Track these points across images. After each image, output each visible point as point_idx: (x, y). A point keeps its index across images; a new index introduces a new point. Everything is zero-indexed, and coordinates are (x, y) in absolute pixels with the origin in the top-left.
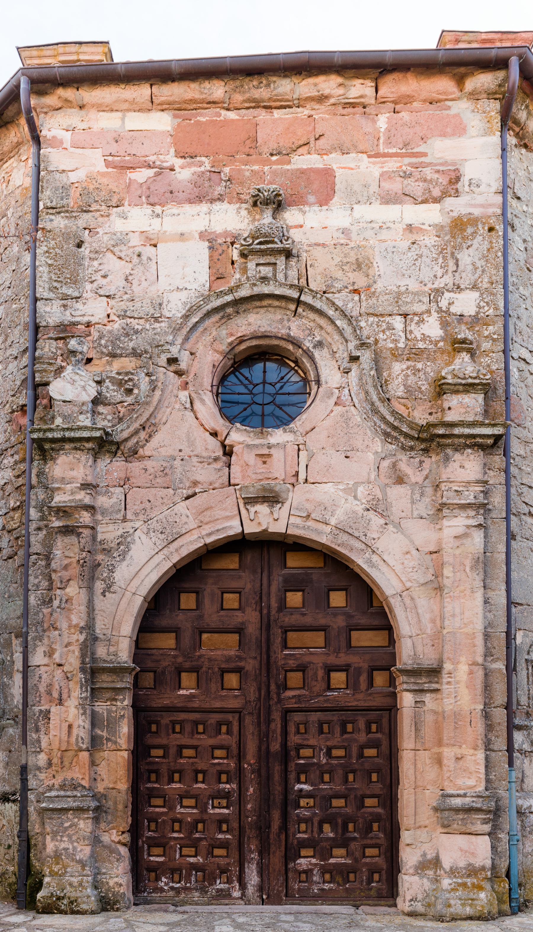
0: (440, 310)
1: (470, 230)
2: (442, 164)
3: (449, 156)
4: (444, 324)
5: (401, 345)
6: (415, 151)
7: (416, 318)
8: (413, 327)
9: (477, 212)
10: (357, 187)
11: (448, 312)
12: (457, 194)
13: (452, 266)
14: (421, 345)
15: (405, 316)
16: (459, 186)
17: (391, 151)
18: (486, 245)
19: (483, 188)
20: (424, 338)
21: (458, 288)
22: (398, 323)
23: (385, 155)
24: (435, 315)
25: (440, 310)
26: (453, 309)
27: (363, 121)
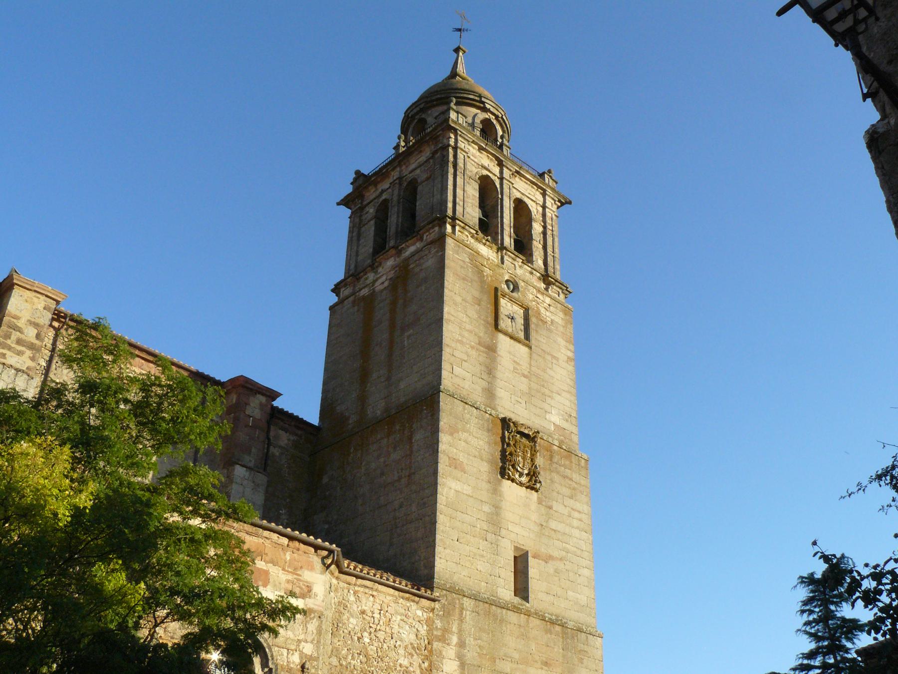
0: (300, 651)
1: (313, 615)
2: (306, 582)
3: (309, 579)
4: (301, 658)
5: (285, 664)
6: (298, 573)
7: (291, 652)
8: (290, 656)
9: (316, 608)
10: (277, 583)
11: (302, 651)
12: (310, 597)
13: (305, 631)
14: (292, 666)
15: (288, 650)
16: (311, 594)
17: (290, 570)
18: (317, 624)
19: (318, 598)
20: (294, 662)
21: (306, 641)
22: (285, 652)
23: (288, 571)
24: (298, 652)
25: (300, 651)
26: (304, 651)
27: (282, 554)
